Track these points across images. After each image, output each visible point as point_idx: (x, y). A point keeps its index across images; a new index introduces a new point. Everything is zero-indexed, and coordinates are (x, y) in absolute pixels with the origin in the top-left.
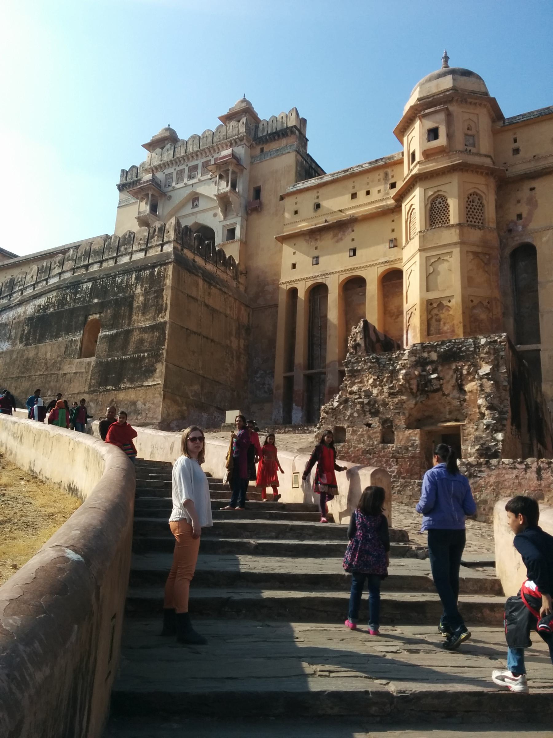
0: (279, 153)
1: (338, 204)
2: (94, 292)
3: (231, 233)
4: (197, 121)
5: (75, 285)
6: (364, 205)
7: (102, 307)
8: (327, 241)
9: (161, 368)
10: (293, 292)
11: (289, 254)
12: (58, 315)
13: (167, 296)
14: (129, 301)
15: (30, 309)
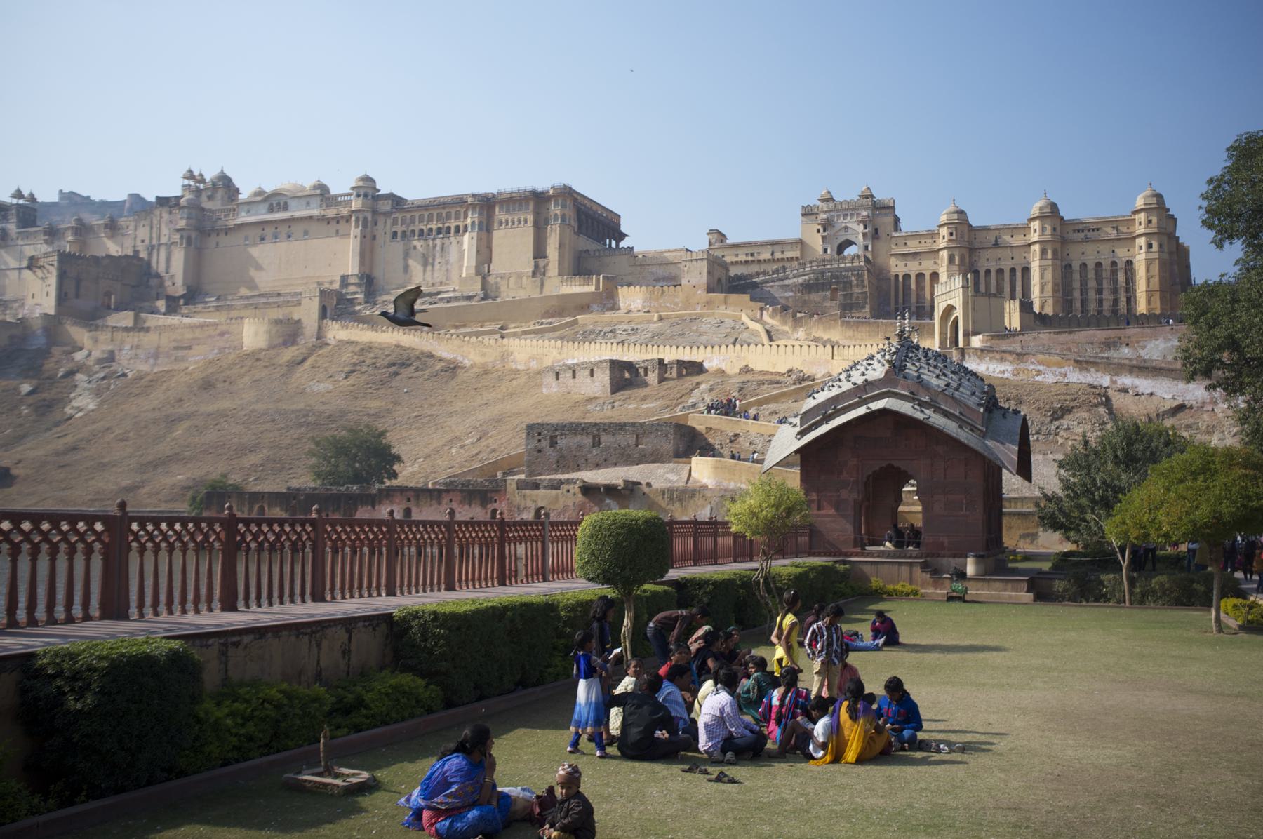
0: (886, 215)
1: (913, 246)
2: (832, 277)
3: (866, 247)
4: (847, 193)
5: (823, 273)
6: (923, 248)
7: (837, 283)
8: (910, 258)
9: (868, 306)
10: (897, 276)
11: (893, 261)
12: (817, 284)
13: (866, 282)
14: (850, 282)
15: (800, 280)
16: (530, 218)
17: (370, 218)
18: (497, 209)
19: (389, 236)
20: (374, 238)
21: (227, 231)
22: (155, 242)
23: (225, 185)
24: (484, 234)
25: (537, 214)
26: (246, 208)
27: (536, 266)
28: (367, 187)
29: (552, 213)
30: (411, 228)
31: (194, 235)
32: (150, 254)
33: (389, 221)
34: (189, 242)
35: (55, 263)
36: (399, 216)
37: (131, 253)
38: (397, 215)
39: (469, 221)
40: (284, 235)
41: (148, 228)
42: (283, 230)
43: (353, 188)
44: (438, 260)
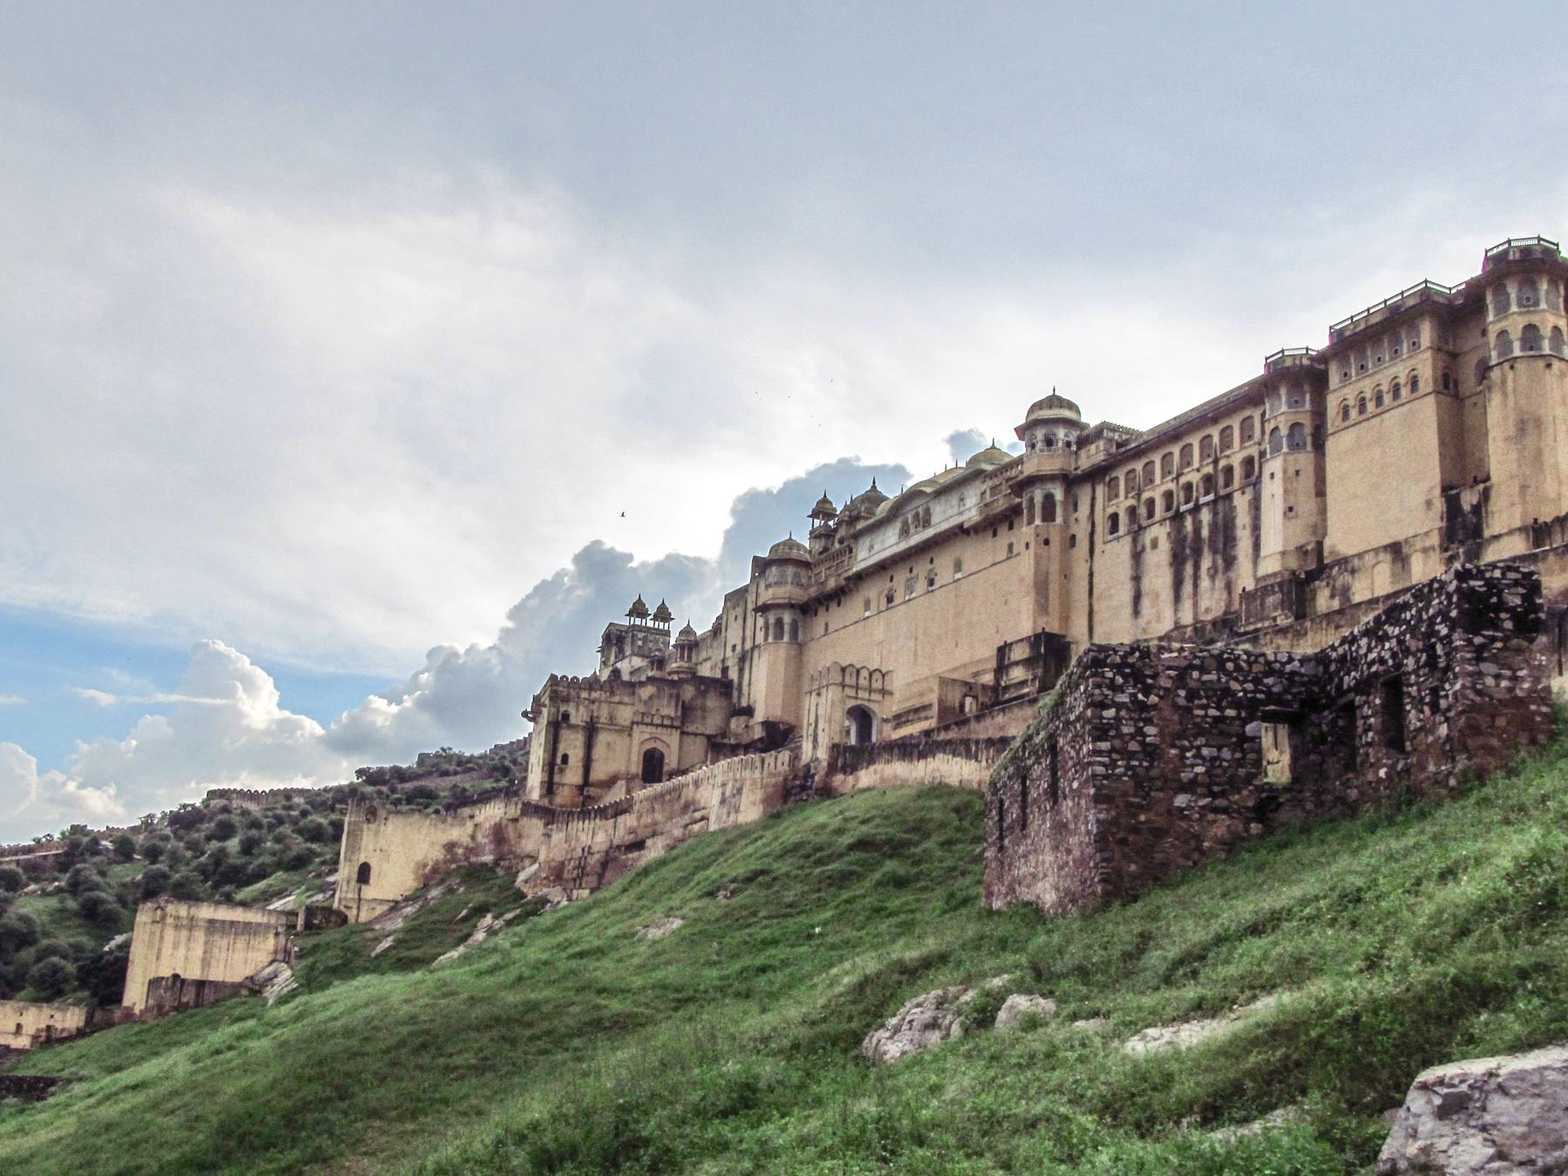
16: (1425, 365)
17: (1059, 494)
18: (1334, 379)
21: (837, 596)
24: (1305, 460)
29: (1493, 331)
31: (787, 618)
32: (741, 670)
34: (779, 635)
37: (718, 675)
40: (921, 586)
41: (740, 621)
42: (922, 568)
43: (1021, 431)
44: (1206, 563)
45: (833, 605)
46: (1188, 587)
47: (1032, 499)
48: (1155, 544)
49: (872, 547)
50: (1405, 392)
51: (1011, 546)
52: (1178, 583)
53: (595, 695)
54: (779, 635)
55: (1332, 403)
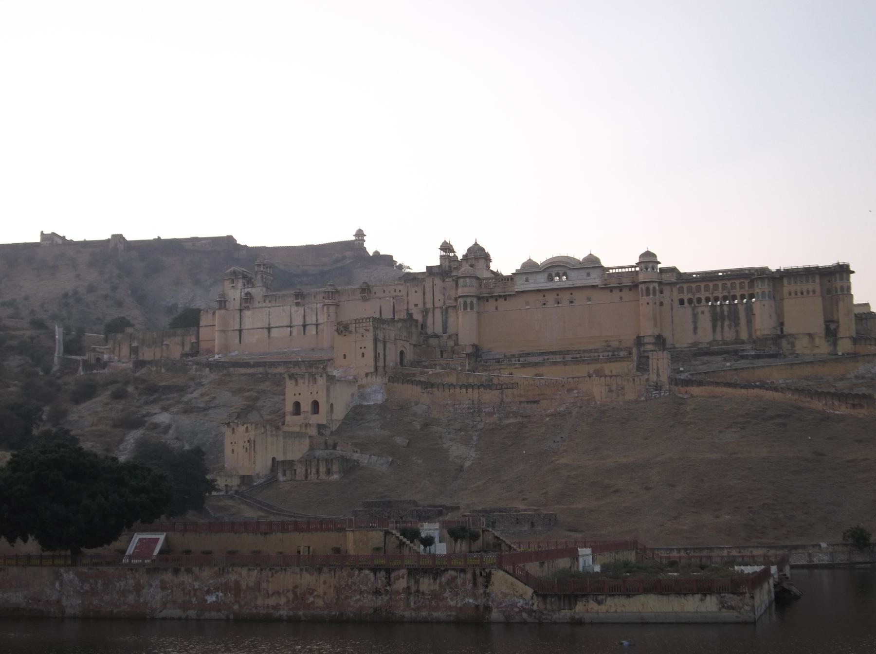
16: (818, 288)
18: (785, 281)
19: (676, 303)
20: (661, 304)
21: (505, 297)
22: (429, 305)
23: (478, 255)
25: (821, 285)
26: (524, 277)
27: (827, 329)
28: (648, 259)
30: (698, 295)
33: (675, 290)
34: (472, 308)
35: (371, 328)
36: (685, 286)
38: (681, 285)
39: (757, 290)
41: (420, 294)
44: (727, 323)
45: (501, 302)
46: (719, 329)
47: (648, 289)
48: (703, 312)
49: (527, 280)
50: (811, 293)
51: (621, 298)
52: (714, 328)
53: (385, 326)
54: (472, 308)
55: (786, 290)
